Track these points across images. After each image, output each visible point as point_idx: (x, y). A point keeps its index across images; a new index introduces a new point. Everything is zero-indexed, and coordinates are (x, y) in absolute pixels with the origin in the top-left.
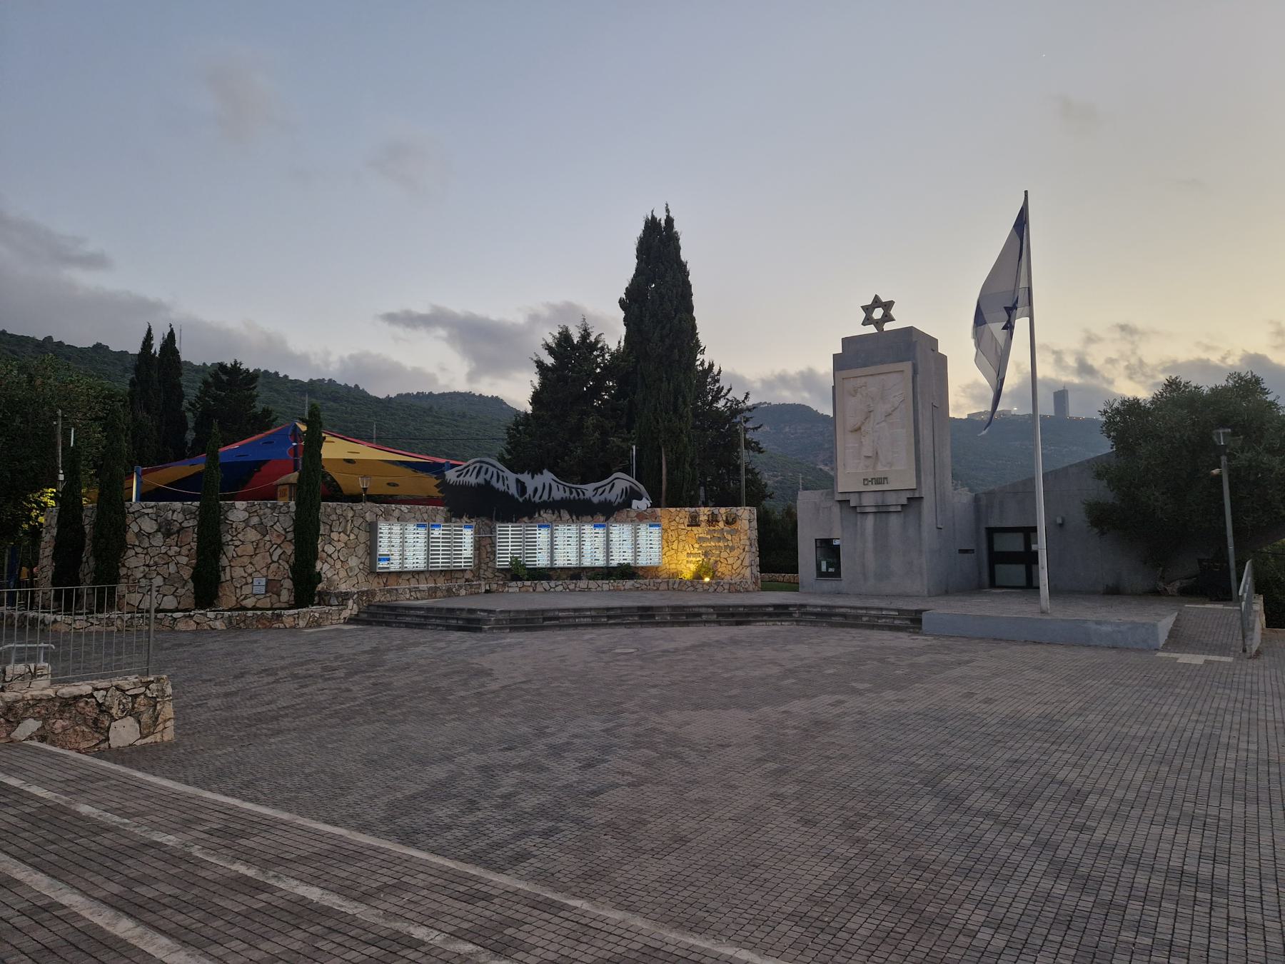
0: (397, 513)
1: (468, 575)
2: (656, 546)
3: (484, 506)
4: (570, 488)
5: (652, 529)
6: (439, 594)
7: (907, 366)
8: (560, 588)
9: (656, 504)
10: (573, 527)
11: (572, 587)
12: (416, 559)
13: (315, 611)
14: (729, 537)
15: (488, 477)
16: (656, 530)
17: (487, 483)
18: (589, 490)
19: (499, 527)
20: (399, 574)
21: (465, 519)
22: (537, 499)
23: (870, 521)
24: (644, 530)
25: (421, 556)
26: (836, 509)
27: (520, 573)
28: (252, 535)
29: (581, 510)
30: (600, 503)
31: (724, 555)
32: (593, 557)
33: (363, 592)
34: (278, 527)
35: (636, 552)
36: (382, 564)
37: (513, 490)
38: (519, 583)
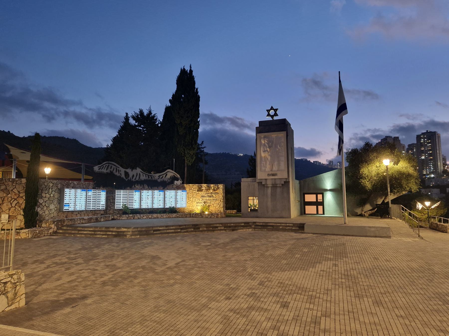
0: (72, 185)
1: (102, 212)
2: (184, 198)
3: (110, 183)
4: (148, 176)
5: (183, 193)
6: (92, 221)
8: (145, 217)
10: (150, 192)
11: (150, 217)
13: (37, 230)
14: (214, 196)
15: (112, 170)
16: (184, 193)
17: (111, 172)
19: (117, 192)
20: (72, 212)
21: (102, 188)
22: (134, 180)
24: (180, 192)
27: (127, 212)
30: (161, 181)
31: (212, 203)
32: (158, 205)
33: (59, 221)
36: (66, 208)
37: (123, 176)
38: (127, 216)
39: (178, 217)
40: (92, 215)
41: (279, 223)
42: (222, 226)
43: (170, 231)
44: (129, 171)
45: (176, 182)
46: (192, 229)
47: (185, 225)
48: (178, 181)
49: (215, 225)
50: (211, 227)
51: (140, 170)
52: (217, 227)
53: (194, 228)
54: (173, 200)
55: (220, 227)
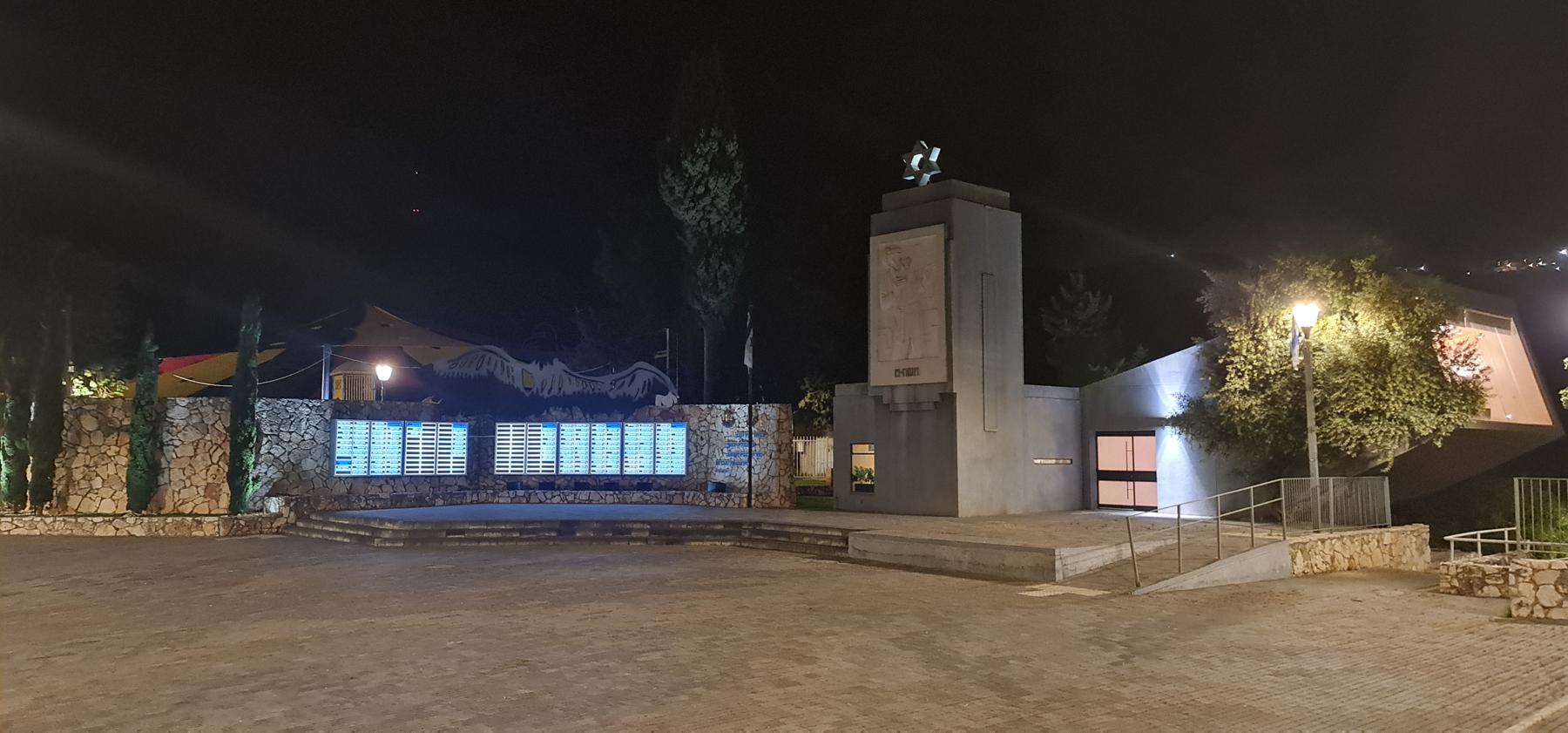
1: (461, 483)
5: (674, 430)
7: (940, 229)
8: (557, 499)
10: (584, 427)
11: (570, 498)
12: (386, 462)
18: (605, 384)
22: (545, 394)
23: (903, 422)
24: (665, 428)
25: (397, 457)
28: (192, 435)
29: (594, 408)
32: (605, 465)
37: (518, 384)
39: (646, 502)
40: (407, 490)
41: (808, 527)
44: (533, 368)
45: (659, 399)
49: (629, 526)
52: (629, 531)
53: (560, 532)
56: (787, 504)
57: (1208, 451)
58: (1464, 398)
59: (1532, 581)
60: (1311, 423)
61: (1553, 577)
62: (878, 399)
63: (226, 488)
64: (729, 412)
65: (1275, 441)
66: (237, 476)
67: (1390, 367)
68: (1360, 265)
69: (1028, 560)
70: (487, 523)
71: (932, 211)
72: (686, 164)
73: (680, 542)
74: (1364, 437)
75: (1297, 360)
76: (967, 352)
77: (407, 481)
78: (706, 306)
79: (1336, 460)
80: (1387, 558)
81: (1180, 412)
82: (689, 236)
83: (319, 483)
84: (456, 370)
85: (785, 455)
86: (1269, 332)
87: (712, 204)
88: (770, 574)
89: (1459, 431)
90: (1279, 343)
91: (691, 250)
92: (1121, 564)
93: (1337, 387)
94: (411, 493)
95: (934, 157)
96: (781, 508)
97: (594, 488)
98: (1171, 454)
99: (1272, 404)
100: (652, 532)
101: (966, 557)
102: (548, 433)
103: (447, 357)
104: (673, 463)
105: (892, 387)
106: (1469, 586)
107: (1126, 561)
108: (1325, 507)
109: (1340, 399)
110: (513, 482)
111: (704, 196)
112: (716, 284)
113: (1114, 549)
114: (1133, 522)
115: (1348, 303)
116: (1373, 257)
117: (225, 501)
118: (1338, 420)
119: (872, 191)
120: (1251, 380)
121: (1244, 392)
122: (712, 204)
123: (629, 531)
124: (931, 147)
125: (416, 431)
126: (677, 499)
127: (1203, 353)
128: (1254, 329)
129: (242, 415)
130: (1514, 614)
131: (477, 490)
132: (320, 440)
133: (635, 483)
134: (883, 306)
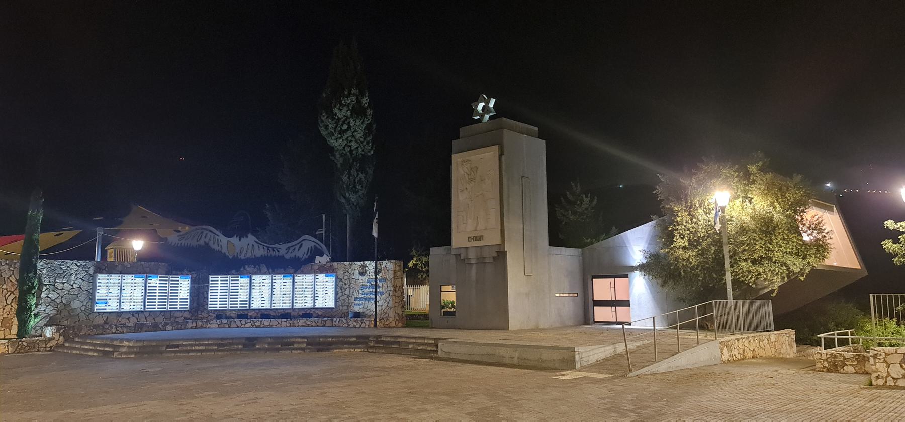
1: (186, 315)
5: (327, 279)
7: (496, 148)
8: (249, 325)
9: (333, 260)
10: (268, 278)
11: (258, 324)
17: (206, 244)
18: (282, 249)
24: (321, 277)
25: (140, 299)
26: (453, 260)
32: (282, 302)
34: (13, 279)
35: (315, 297)
37: (224, 251)
38: (218, 321)
42: (302, 343)
43: (200, 348)
44: (234, 240)
45: (318, 259)
46: (241, 347)
47: (232, 339)
48: (322, 255)
50: (278, 344)
51: (255, 239)
52: (293, 343)
53: (245, 345)
54: (309, 293)
55: (299, 343)
56: (400, 324)
57: (662, 286)
58: (817, 250)
59: (885, 361)
60: (727, 266)
61: (899, 358)
62: (457, 256)
63: (15, 320)
64: (363, 267)
65: (704, 278)
66: (23, 312)
67: (774, 230)
68: (753, 168)
69: (556, 356)
70: (195, 340)
71: (491, 138)
72: (336, 111)
73: (328, 350)
74: (760, 274)
75: (718, 227)
76: (514, 225)
77: (147, 314)
78: (348, 200)
79: (744, 290)
80: (773, 350)
81: (644, 262)
82: (338, 156)
83: (83, 316)
84: (183, 242)
85: (399, 293)
86: (700, 210)
87: (353, 136)
88: (384, 369)
89: (814, 271)
90: (706, 218)
91: (339, 166)
92: (617, 356)
93: (742, 243)
94: (150, 322)
95: (491, 105)
96: (396, 327)
97: (274, 317)
98: (639, 287)
99: (702, 255)
100: (308, 344)
101: (517, 355)
102: (244, 282)
103: (179, 234)
104: (327, 300)
105: (467, 248)
106: (834, 367)
107: (620, 355)
108: (737, 317)
109: (745, 250)
110: (220, 314)
111: (347, 131)
112: (355, 186)
113: (611, 347)
114: (623, 331)
115: (746, 192)
116: (760, 164)
117: (14, 330)
118: (744, 264)
119: (450, 126)
120: (689, 240)
121: (685, 248)
122: (353, 136)
123: (293, 343)
124: (489, 98)
125: (155, 281)
126: (329, 323)
127: (659, 225)
128: (690, 210)
129: (27, 268)
130: (874, 383)
131: (195, 320)
132: (85, 288)
133: (301, 313)
134: (460, 197)
